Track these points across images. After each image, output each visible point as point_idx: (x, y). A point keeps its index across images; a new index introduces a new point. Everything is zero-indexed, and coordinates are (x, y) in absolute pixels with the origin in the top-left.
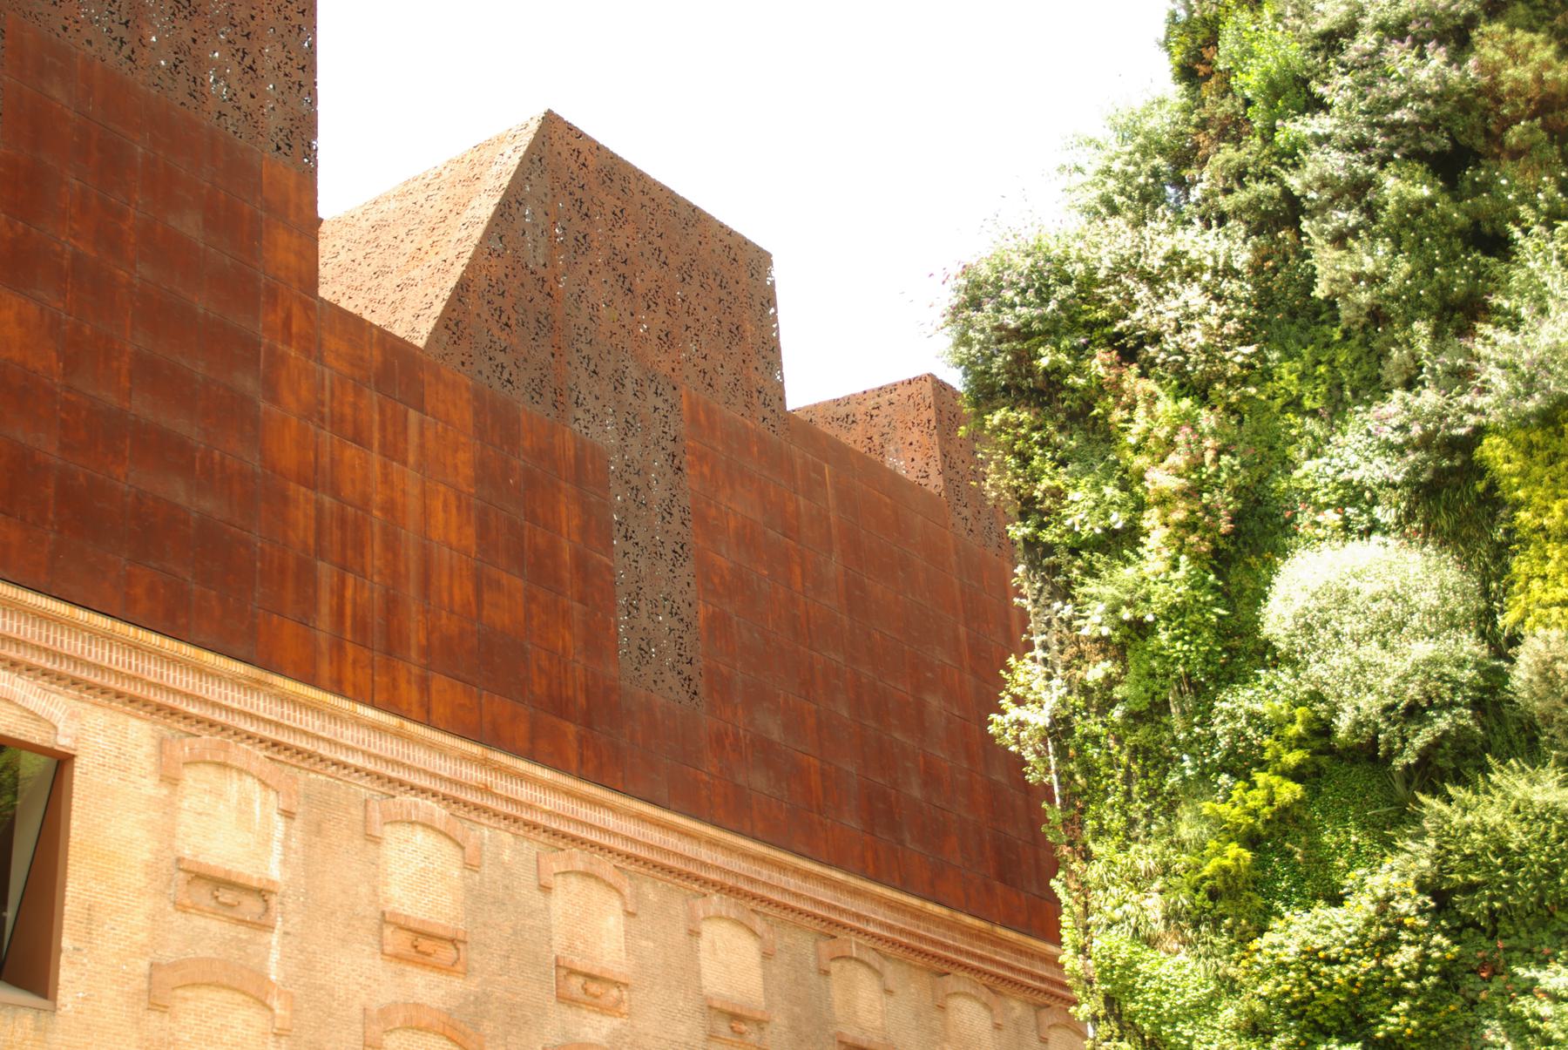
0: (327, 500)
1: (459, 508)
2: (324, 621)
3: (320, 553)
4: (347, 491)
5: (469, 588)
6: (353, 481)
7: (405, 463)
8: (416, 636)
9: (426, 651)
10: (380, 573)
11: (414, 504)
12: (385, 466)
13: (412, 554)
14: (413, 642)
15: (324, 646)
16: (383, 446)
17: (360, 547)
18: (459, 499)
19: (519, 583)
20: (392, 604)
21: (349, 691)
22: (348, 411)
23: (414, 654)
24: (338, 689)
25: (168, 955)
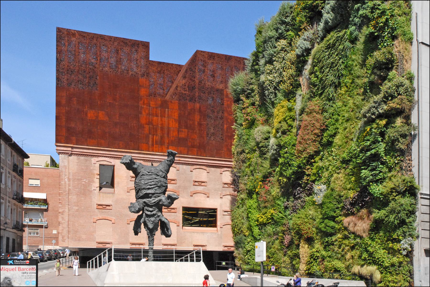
0: (151, 126)
1: (175, 122)
2: (150, 143)
3: (150, 133)
4: (154, 124)
5: (176, 133)
6: (155, 122)
7: (165, 117)
8: (166, 141)
9: (168, 143)
10: (160, 134)
11: (166, 123)
12: (161, 118)
13: (166, 130)
14: (166, 142)
15: (150, 146)
16: (161, 115)
17: (156, 131)
18: (175, 120)
19: (186, 130)
20: (162, 138)
21: (155, 151)
22: (155, 112)
23: (166, 144)
24: (153, 151)
25: (129, 186)
